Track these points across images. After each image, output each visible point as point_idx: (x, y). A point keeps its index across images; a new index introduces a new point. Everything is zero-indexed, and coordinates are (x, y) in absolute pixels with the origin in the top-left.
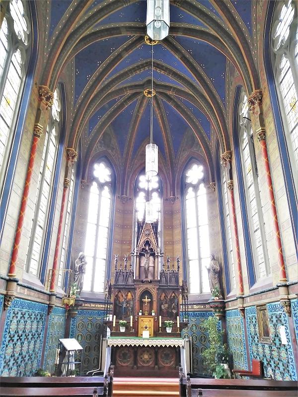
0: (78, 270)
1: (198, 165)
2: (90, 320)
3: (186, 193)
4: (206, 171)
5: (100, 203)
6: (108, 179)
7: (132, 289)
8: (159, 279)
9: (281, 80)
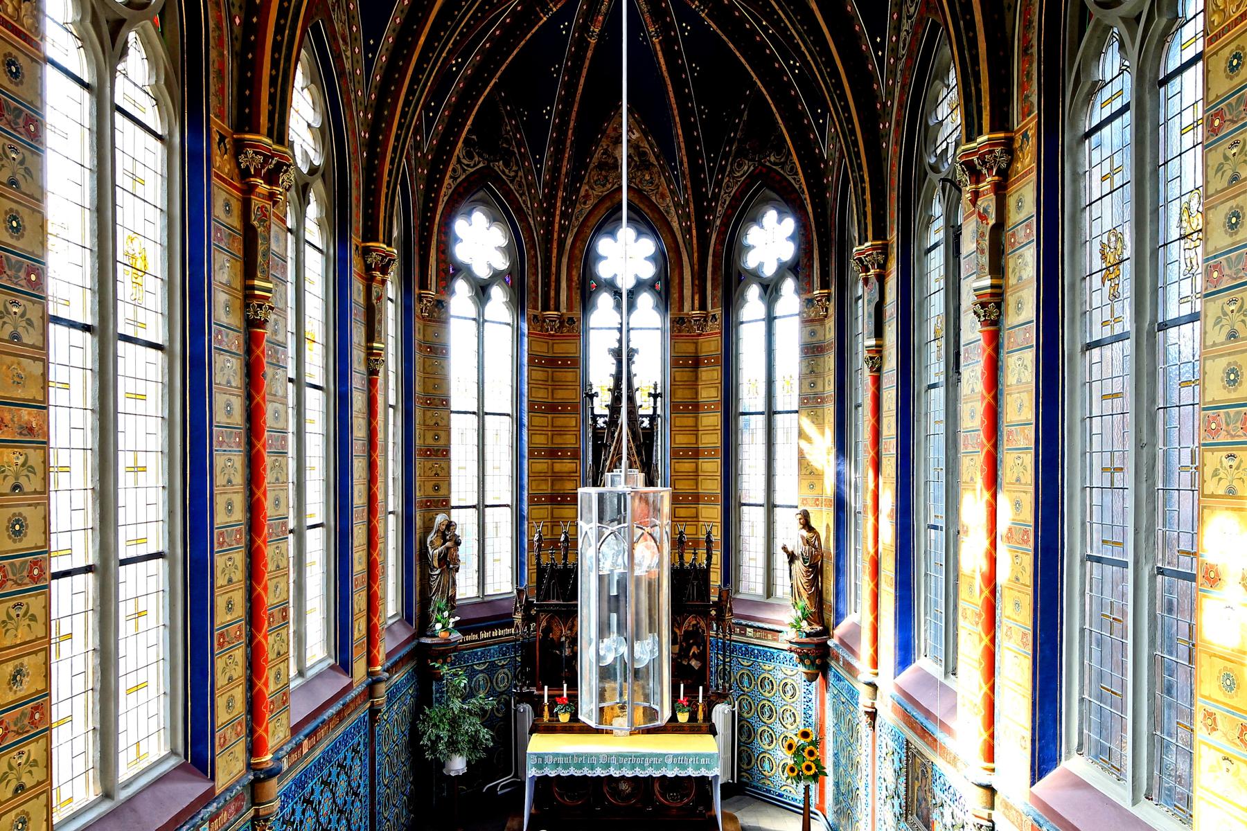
0: (436, 564)
1: (780, 213)
3: (742, 298)
4: (803, 237)
5: (482, 349)
6: (502, 263)
9: (1095, 122)
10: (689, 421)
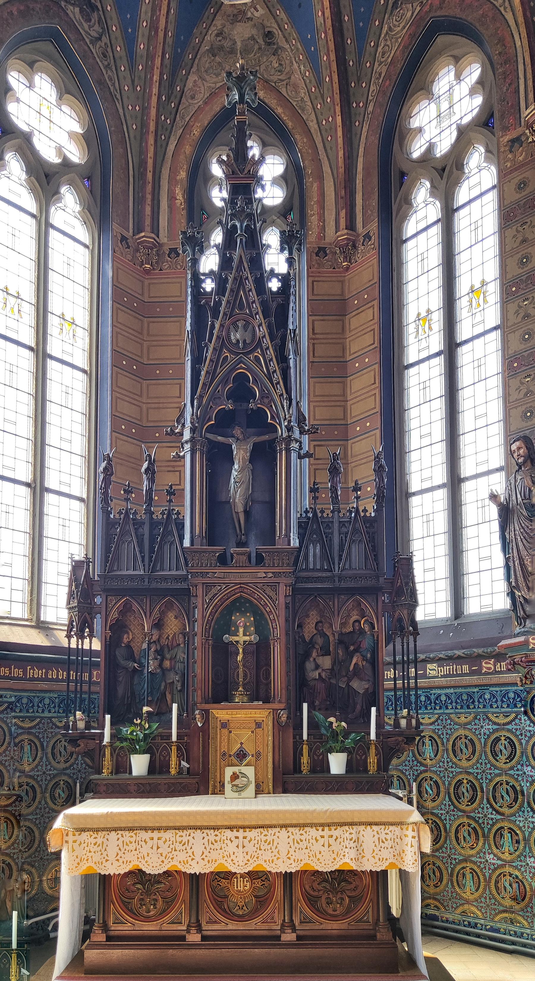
2: (28, 731)
6: (76, 155)
7: (184, 596)
8: (295, 542)
10: (336, 389)
